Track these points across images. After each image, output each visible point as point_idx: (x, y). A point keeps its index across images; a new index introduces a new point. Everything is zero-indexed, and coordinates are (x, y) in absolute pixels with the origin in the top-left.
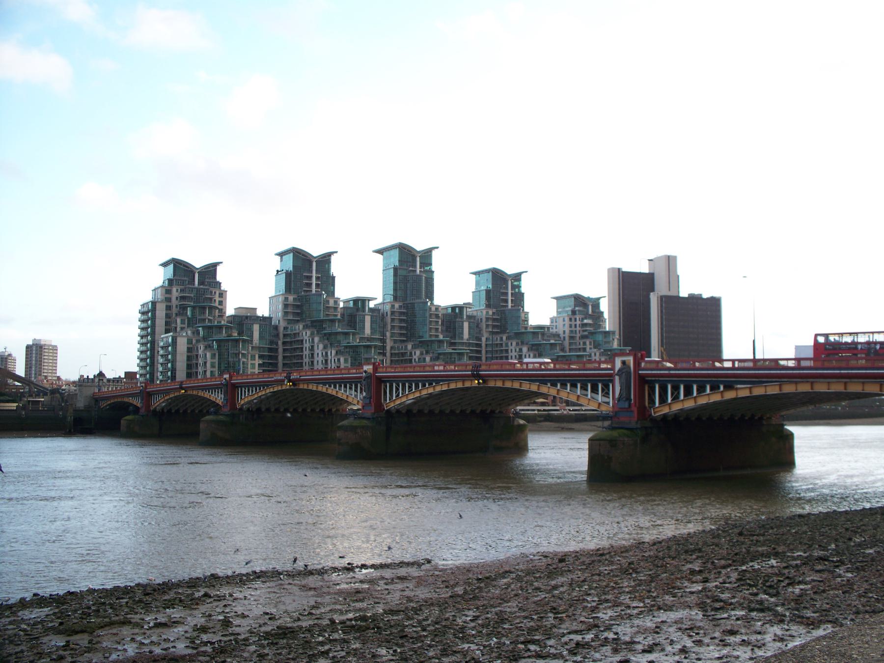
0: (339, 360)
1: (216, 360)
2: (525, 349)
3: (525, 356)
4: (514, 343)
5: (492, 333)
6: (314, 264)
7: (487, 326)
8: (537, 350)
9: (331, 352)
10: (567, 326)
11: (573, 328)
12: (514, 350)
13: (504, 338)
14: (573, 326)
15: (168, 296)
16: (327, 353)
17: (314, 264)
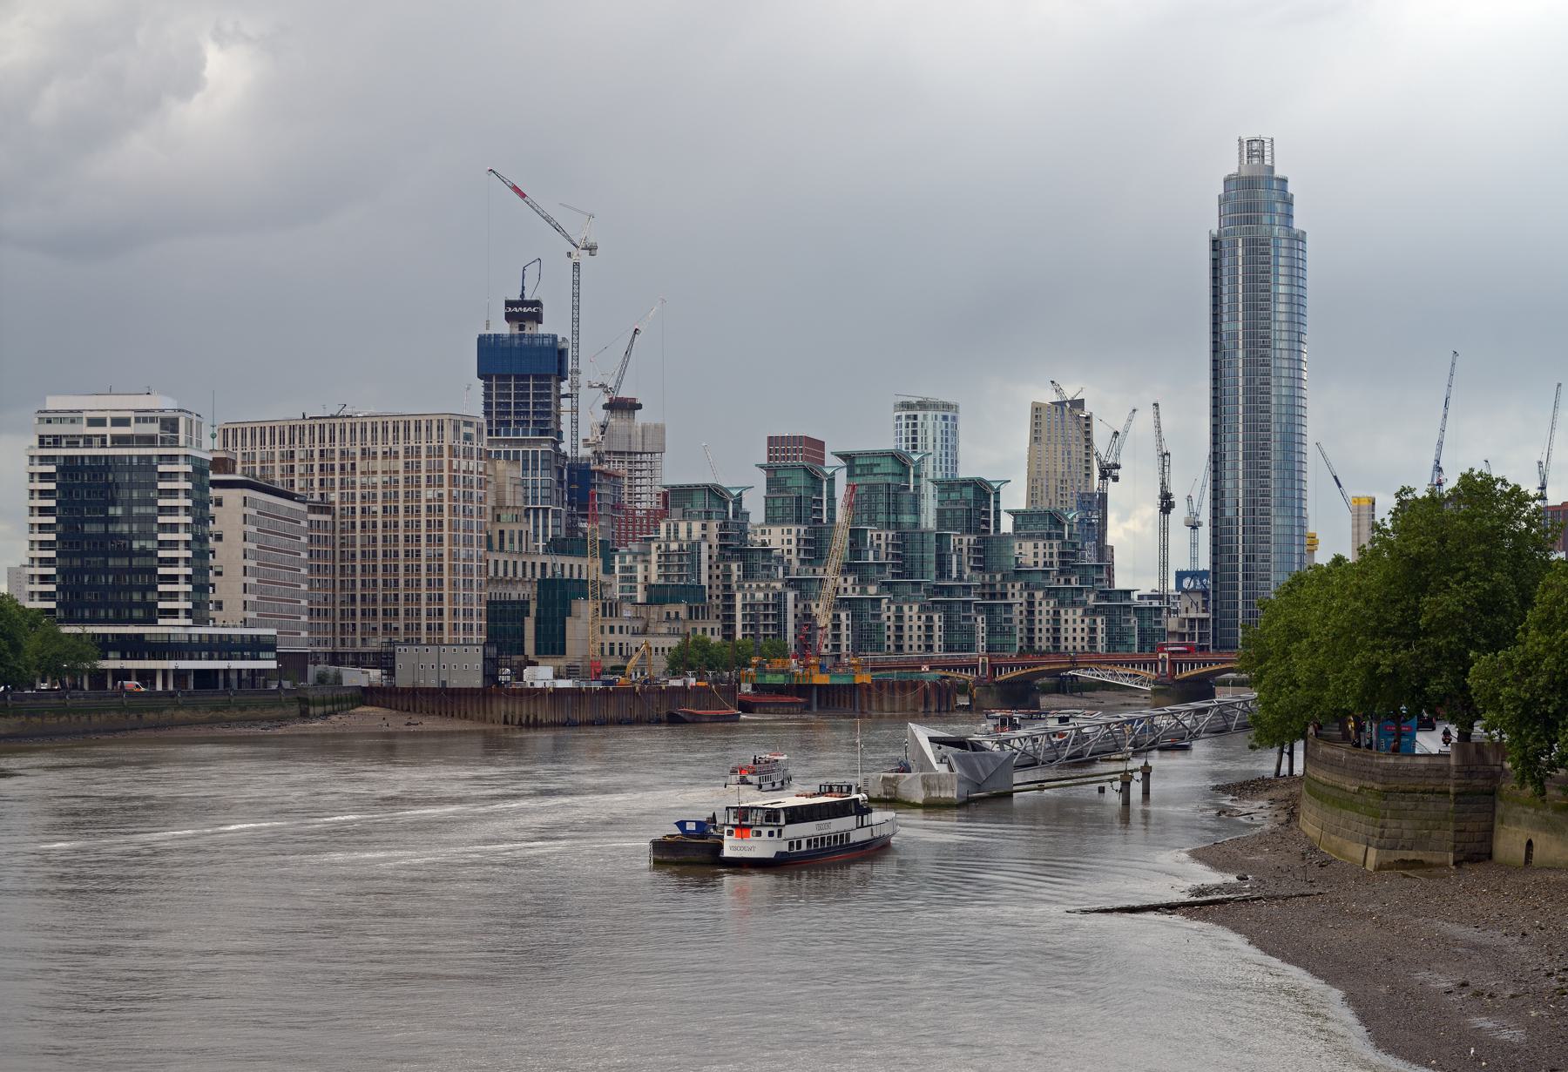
0: (929, 619)
1: (850, 622)
2: (1039, 595)
3: (1040, 604)
4: (1018, 586)
5: (973, 568)
6: (825, 484)
7: (969, 558)
8: (1056, 596)
9: (911, 608)
10: (1041, 555)
11: (1047, 559)
12: (1017, 595)
13: (998, 577)
14: (1047, 555)
15: (704, 532)
16: (900, 609)
17: (825, 484)
